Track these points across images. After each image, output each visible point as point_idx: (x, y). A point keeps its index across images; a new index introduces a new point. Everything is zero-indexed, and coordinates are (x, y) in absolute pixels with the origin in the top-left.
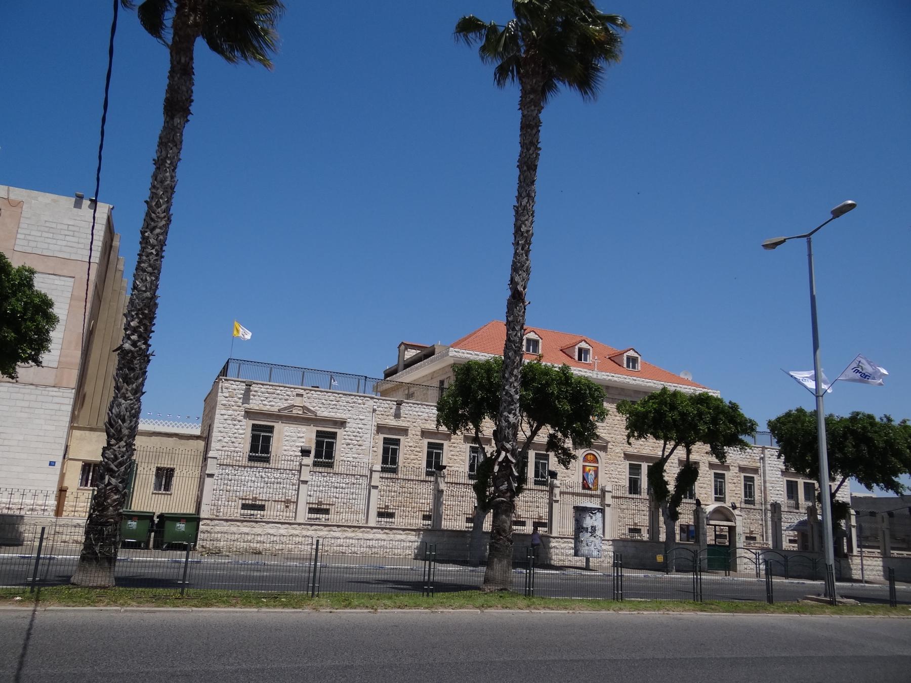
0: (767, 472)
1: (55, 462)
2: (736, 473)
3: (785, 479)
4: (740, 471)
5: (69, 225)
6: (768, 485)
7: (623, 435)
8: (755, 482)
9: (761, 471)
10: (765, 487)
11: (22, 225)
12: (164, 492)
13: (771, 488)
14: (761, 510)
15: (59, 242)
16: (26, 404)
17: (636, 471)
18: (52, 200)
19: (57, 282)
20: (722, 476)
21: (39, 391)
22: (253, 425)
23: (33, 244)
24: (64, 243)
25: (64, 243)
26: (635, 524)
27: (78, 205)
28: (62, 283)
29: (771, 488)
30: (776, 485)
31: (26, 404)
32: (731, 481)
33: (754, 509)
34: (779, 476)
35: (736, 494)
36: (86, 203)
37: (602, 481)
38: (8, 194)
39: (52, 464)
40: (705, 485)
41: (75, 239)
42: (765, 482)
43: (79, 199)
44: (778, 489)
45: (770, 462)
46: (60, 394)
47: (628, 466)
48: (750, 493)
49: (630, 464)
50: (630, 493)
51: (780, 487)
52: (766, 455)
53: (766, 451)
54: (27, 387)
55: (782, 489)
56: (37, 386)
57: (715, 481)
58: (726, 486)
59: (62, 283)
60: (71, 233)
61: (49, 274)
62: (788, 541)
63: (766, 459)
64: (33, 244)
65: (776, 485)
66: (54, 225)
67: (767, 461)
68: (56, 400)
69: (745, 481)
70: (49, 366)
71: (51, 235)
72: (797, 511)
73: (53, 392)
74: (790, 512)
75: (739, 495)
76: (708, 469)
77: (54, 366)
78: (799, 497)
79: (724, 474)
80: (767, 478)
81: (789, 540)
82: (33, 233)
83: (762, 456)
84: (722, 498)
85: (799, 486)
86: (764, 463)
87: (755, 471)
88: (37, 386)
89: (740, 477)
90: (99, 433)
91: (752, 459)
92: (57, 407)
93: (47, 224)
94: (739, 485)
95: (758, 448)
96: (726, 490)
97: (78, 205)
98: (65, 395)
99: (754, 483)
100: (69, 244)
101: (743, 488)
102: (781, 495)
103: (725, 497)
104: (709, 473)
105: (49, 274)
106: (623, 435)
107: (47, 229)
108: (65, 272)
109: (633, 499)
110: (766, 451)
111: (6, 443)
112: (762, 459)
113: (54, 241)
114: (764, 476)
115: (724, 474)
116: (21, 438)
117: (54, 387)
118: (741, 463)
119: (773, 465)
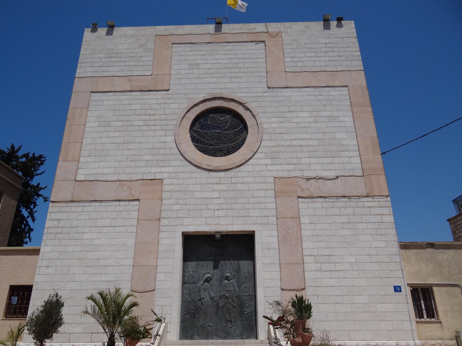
1: (400, 287)
5: (326, 43)
11: (286, 51)
12: (428, 320)
15: (323, 59)
16: (345, 219)
18: (304, 26)
19: (333, 93)
21: (353, 202)
23: (299, 64)
24: (327, 59)
25: (327, 59)
27: (327, 27)
28: (338, 93)
31: (345, 219)
36: (334, 23)
38: (267, 28)
39: (397, 289)
41: (336, 54)
43: (326, 21)
46: (376, 204)
54: (340, 200)
56: (349, 197)
59: (338, 93)
60: (330, 50)
61: (324, 87)
64: (299, 64)
66: (313, 46)
68: (374, 211)
70: (355, 175)
71: (313, 54)
73: (368, 202)
77: (358, 175)
82: (297, 55)
88: (349, 197)
90: (415, 250)
92: (378, 219)
97: (327, 27)
98: (382, 204)
100: (332, 58)
105: (324, 87)
107: (308, 50)
108: (337, 83)
111: (339, 267)
113: (318, 59)
116: (353, 260)
117: (367, 196)
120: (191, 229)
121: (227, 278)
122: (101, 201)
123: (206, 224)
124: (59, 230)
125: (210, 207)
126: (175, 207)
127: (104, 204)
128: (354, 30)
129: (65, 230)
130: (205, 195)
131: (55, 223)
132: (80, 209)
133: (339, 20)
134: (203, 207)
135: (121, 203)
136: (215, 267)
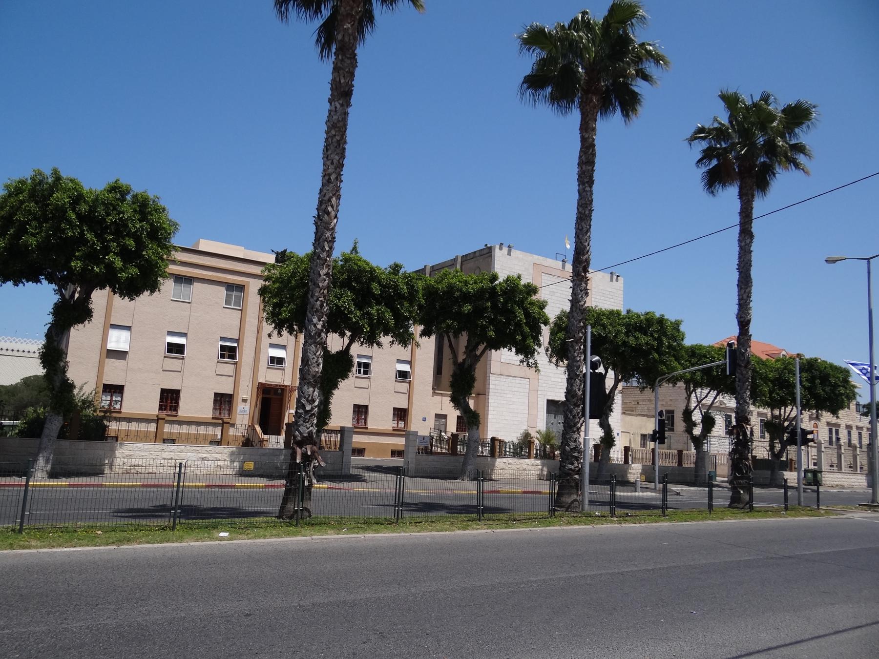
22: (761, 420)
36: (615, 277)
37: (820, 438)
41: (612, 300)
43: (612, 273)
93: (602, 291)
120: (550, 398)
121: (559, 423)
122: (513, 377)
123: (556, 396)
124: (496, 391)
125: (558, 387)
126: (544, 385)
127: (514, 378)
128: (622, 285)
129: (499, 391)
130: (556, 380)
131: (494, 387)
132: (504, 380)
133: (618, 276)
134: (554, 386)
135: (522, 379)
136: (555, 418)
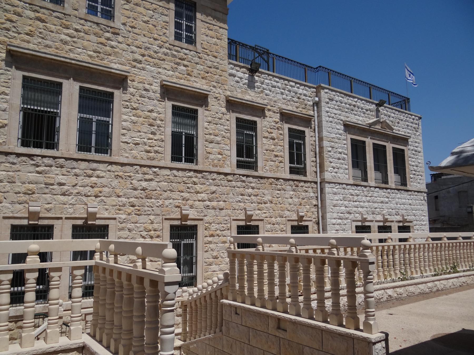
0: (324, 123)
2: (277, 123)
3: (350, 136)
4: (282, 120)
6: (326, 143)
7: (6, 11)
8: (307, 139)
9: (315, 123)
10: (321, 148)
13: (330, 149)
14: (316, 183)
17: (48, 98)
20: (253, 126)
26: (33, 215)
29: (330, 149)
30: (336, 145)
32: (266, 134)
33: (305, 182)
34: (341, 132)
35: (276, 156)
40: (218, 139)
42: (321, 139)
44: (340, 150)
45: (328, 109)
47: (19, 82)
48: (299, 156)
49: (24, 78)
50: (25, 144)
51: (342, 148)
52: (323, 99)
53: (322, 92)
55: (346, 152)
57: (238, 133)
58: (259, 145)
62: (354, 229)
63: (323, 104)
65: (336, 145)
67: (325, 108)
69: (290, 136)
72: (365, 184)
74: (357, 185)
75: (280, 159)
76: (224, 110)
78: (368, 164)
79: (255, 122)
80: (325, 133)
81: (357, 227)
83: (317, 99)
84: (253, 163)
85: (367, 148)
86: (319, 112)
87: (307, 121)
89: (283, 129)
91: (301, 103)
94: (281, 143)
95: (310, 87)
96: (259, 150)
99: (304, 140)
101: (287, 146)
102: (344, 159)
103: (256, 162)
104: (228, 117)
106: (6, 11)
109: (30, 156)
110: (322, 92)
112: (317, 104)
114: (320, 132)
115: (255, 122)
118: (284, 107)
119: (333, 115)
